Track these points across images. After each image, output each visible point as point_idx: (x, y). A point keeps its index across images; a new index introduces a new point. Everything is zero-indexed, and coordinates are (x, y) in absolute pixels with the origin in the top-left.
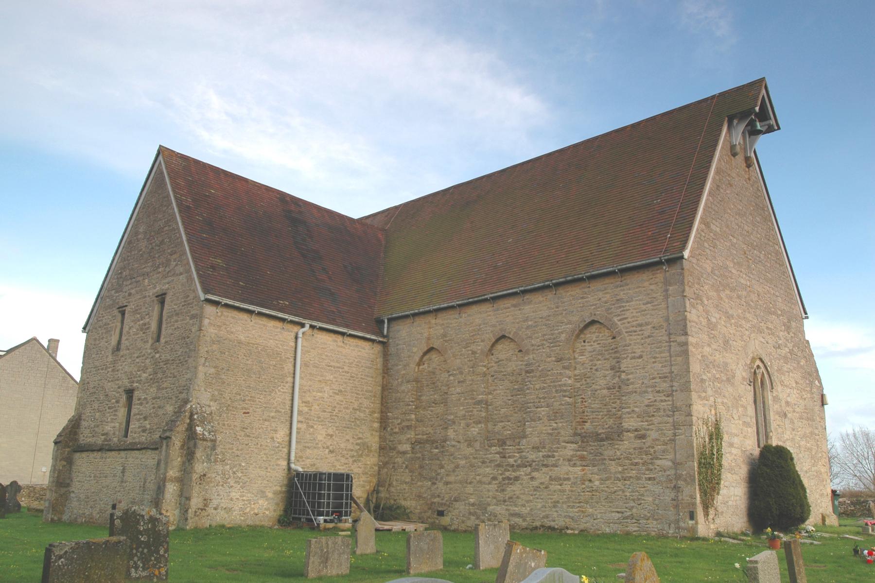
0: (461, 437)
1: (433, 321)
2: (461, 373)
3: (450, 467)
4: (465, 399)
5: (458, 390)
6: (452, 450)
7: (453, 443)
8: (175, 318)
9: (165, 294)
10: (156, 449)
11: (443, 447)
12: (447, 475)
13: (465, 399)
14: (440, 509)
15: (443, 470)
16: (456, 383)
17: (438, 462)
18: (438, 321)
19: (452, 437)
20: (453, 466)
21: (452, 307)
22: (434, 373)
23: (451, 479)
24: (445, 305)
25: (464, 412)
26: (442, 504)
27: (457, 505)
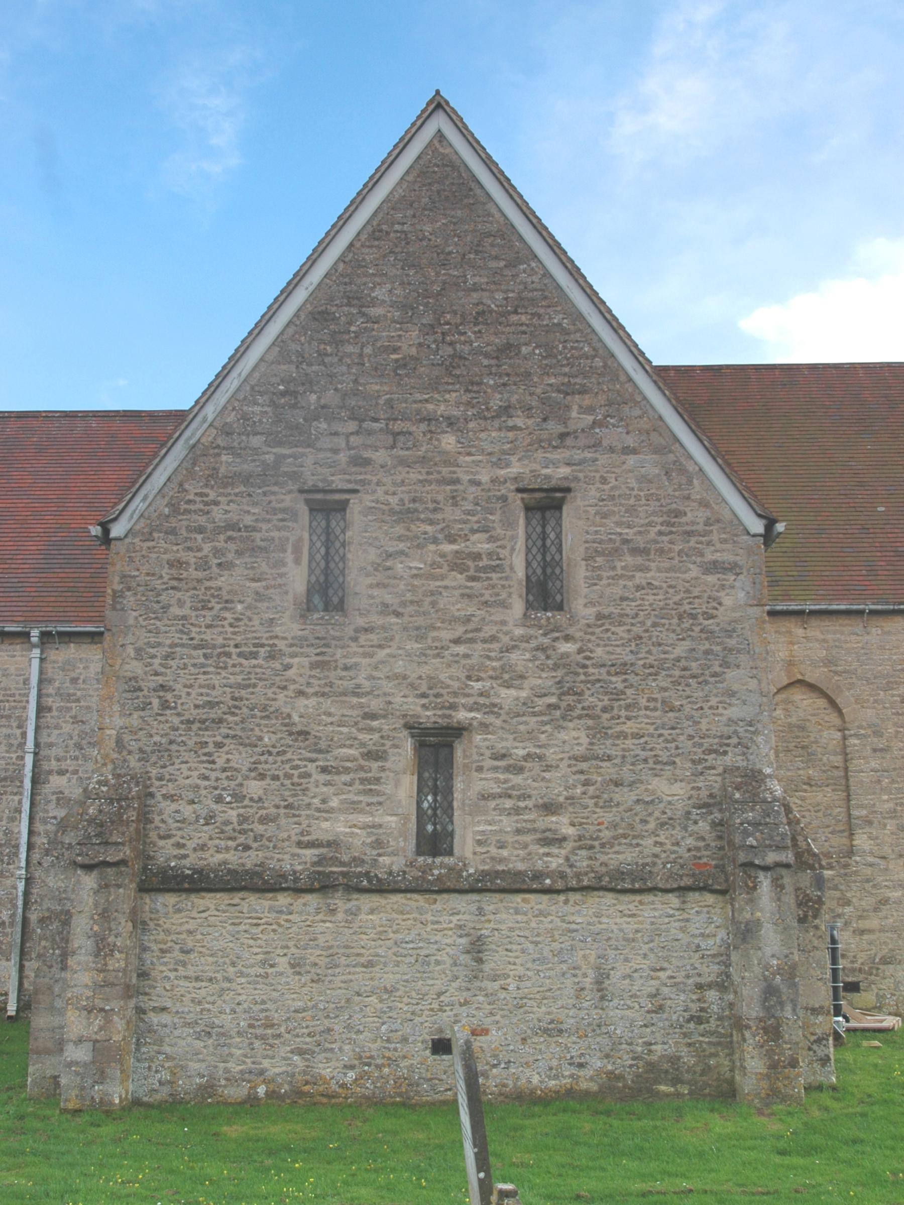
0: (887, 850)
1: (800, 632)
2: (878, 734)
3: (868, 902)
4: (893, 781)
5: (874, 764)
6: (869, 871)
7: (870, 859)
8: (629, 560)
9: (568, 490)
10: (723, 892)
11: (846, 866)
12: (860, 917)
13: (893, 781)
14: (850, 979)
15: (847, 909)
16: (868, 751)
17: (837, 894)
18: (810, 633)
19: (867, 848)
20: (872, 900)
21: (860, 613)
22: (802, 728)
23: (873, 923)
24: (843, 607)
25: (891, 805)
26: (853, 970)
27: (889, 969)
